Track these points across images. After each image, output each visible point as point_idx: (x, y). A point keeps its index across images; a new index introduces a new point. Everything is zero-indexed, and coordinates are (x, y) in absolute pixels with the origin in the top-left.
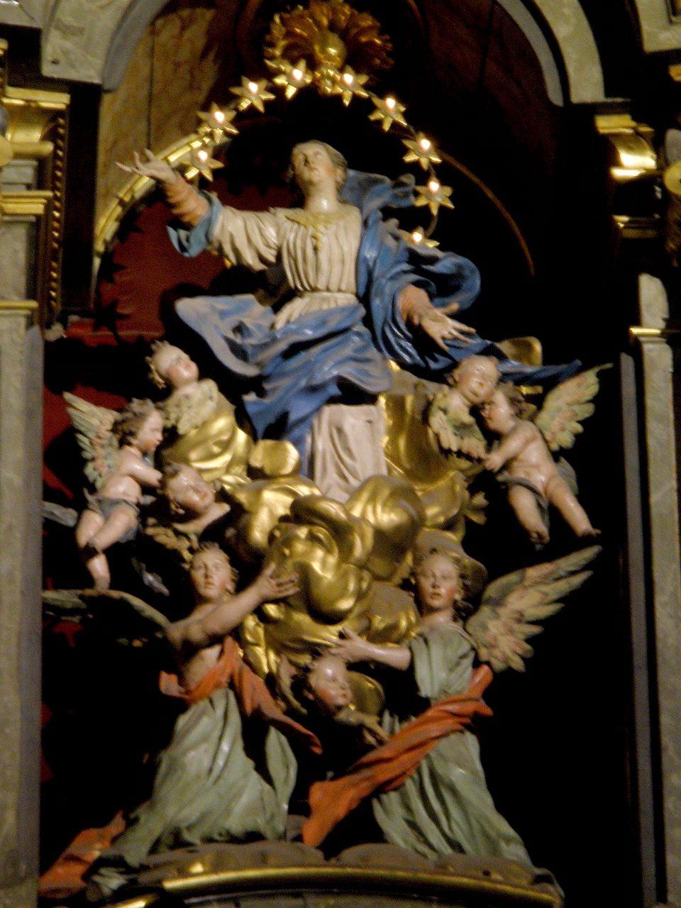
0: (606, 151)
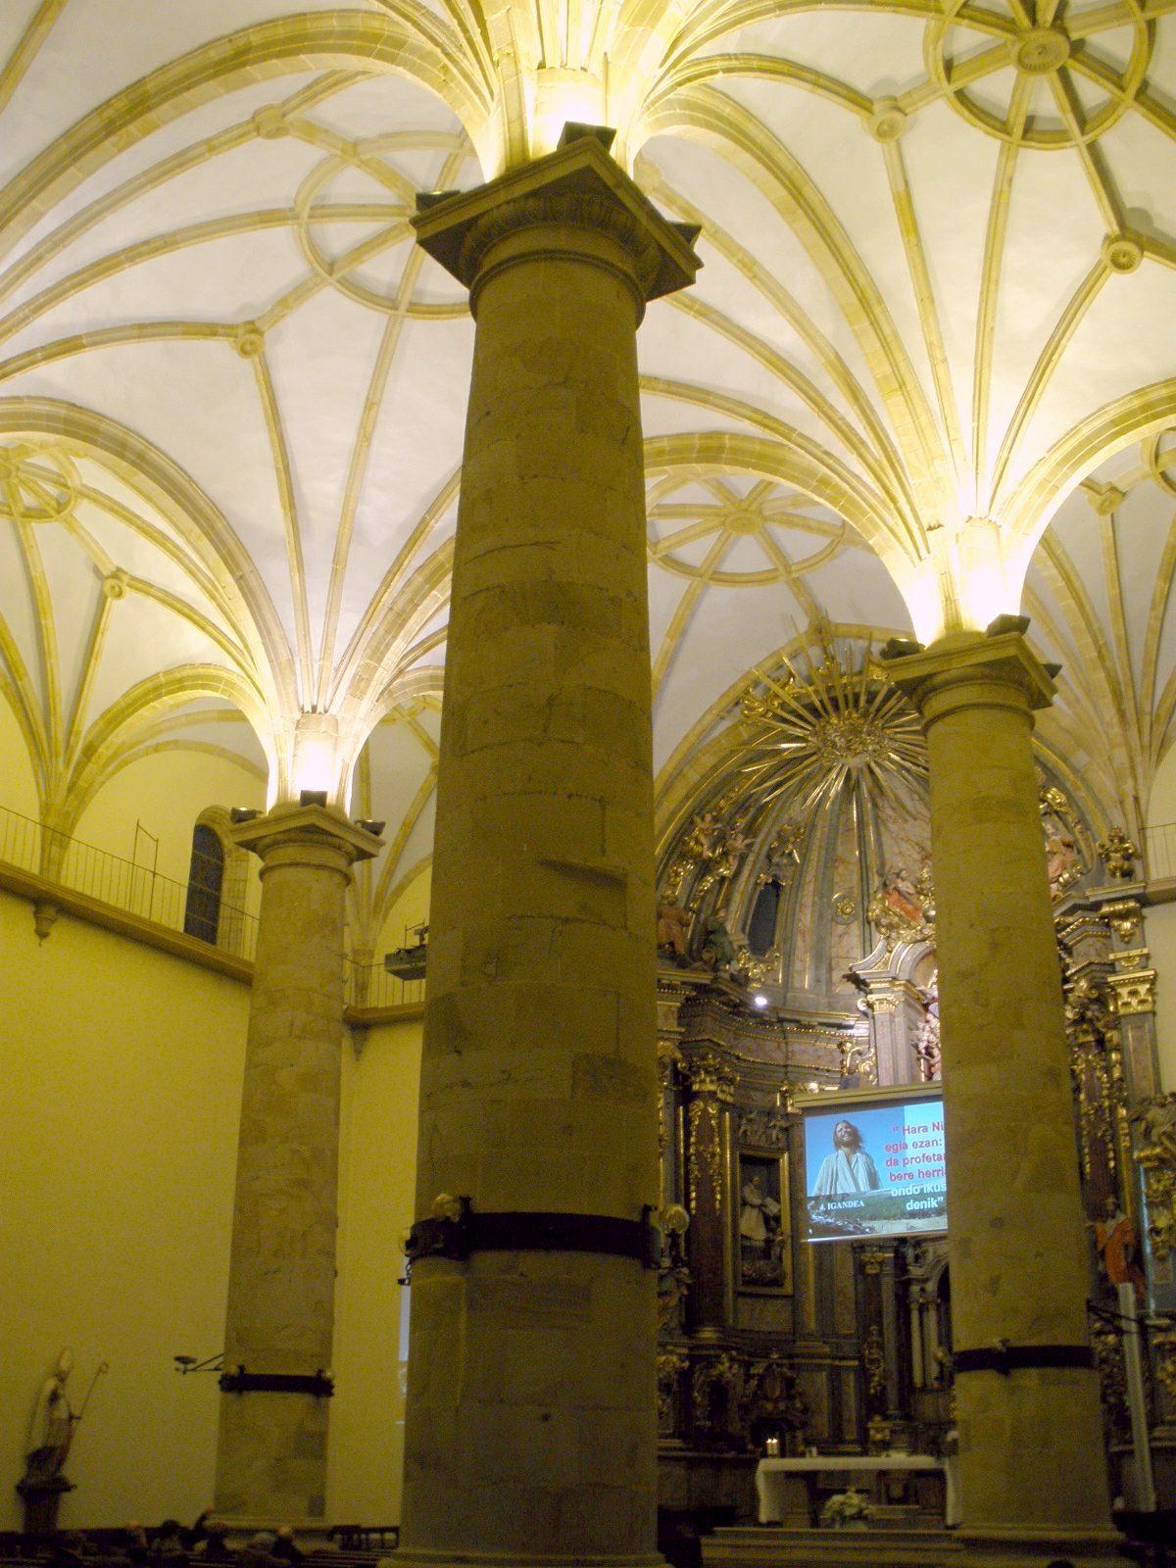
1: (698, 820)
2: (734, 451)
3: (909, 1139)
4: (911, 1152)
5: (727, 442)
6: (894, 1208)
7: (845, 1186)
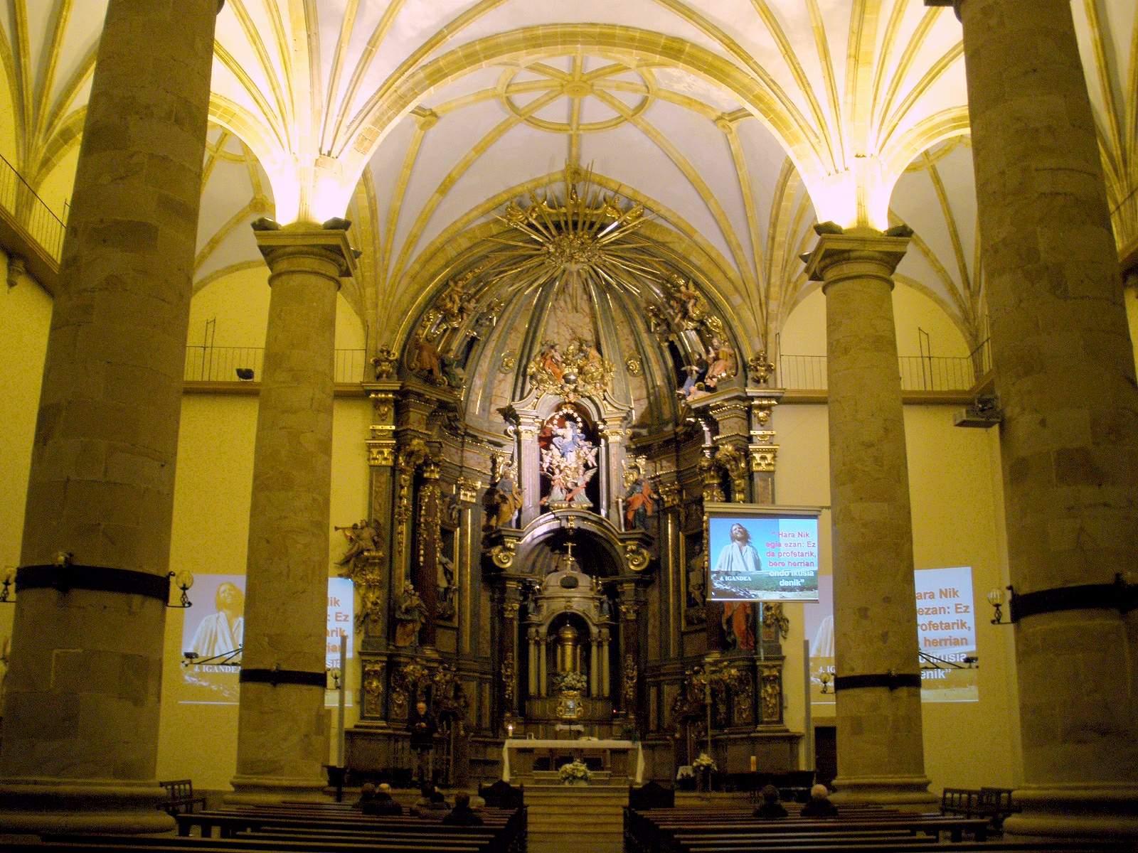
0: (598, 425)
1: (451, 284)
2: (691, 56)
3: (782, 540)
4: (783, 549)
5: (687, 49)
6: (772, 584)
7: (737, 566)
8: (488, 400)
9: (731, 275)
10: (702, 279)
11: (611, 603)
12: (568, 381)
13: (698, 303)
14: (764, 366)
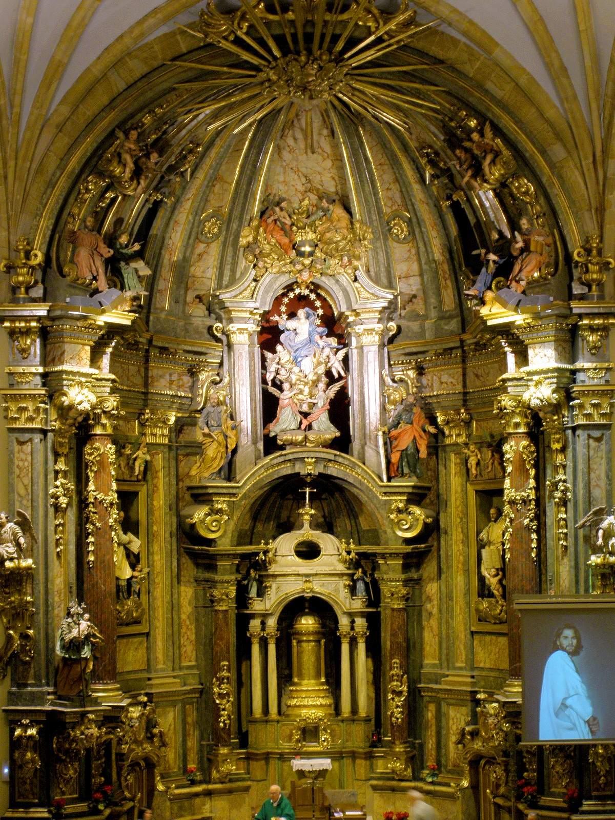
0: (347, 317)
8: (183, 286)
9: (550, 113)
10: (506, 122)
11: (368, 580)
12: (301, 254)
13: (497, 160)
14: (597, 264)
